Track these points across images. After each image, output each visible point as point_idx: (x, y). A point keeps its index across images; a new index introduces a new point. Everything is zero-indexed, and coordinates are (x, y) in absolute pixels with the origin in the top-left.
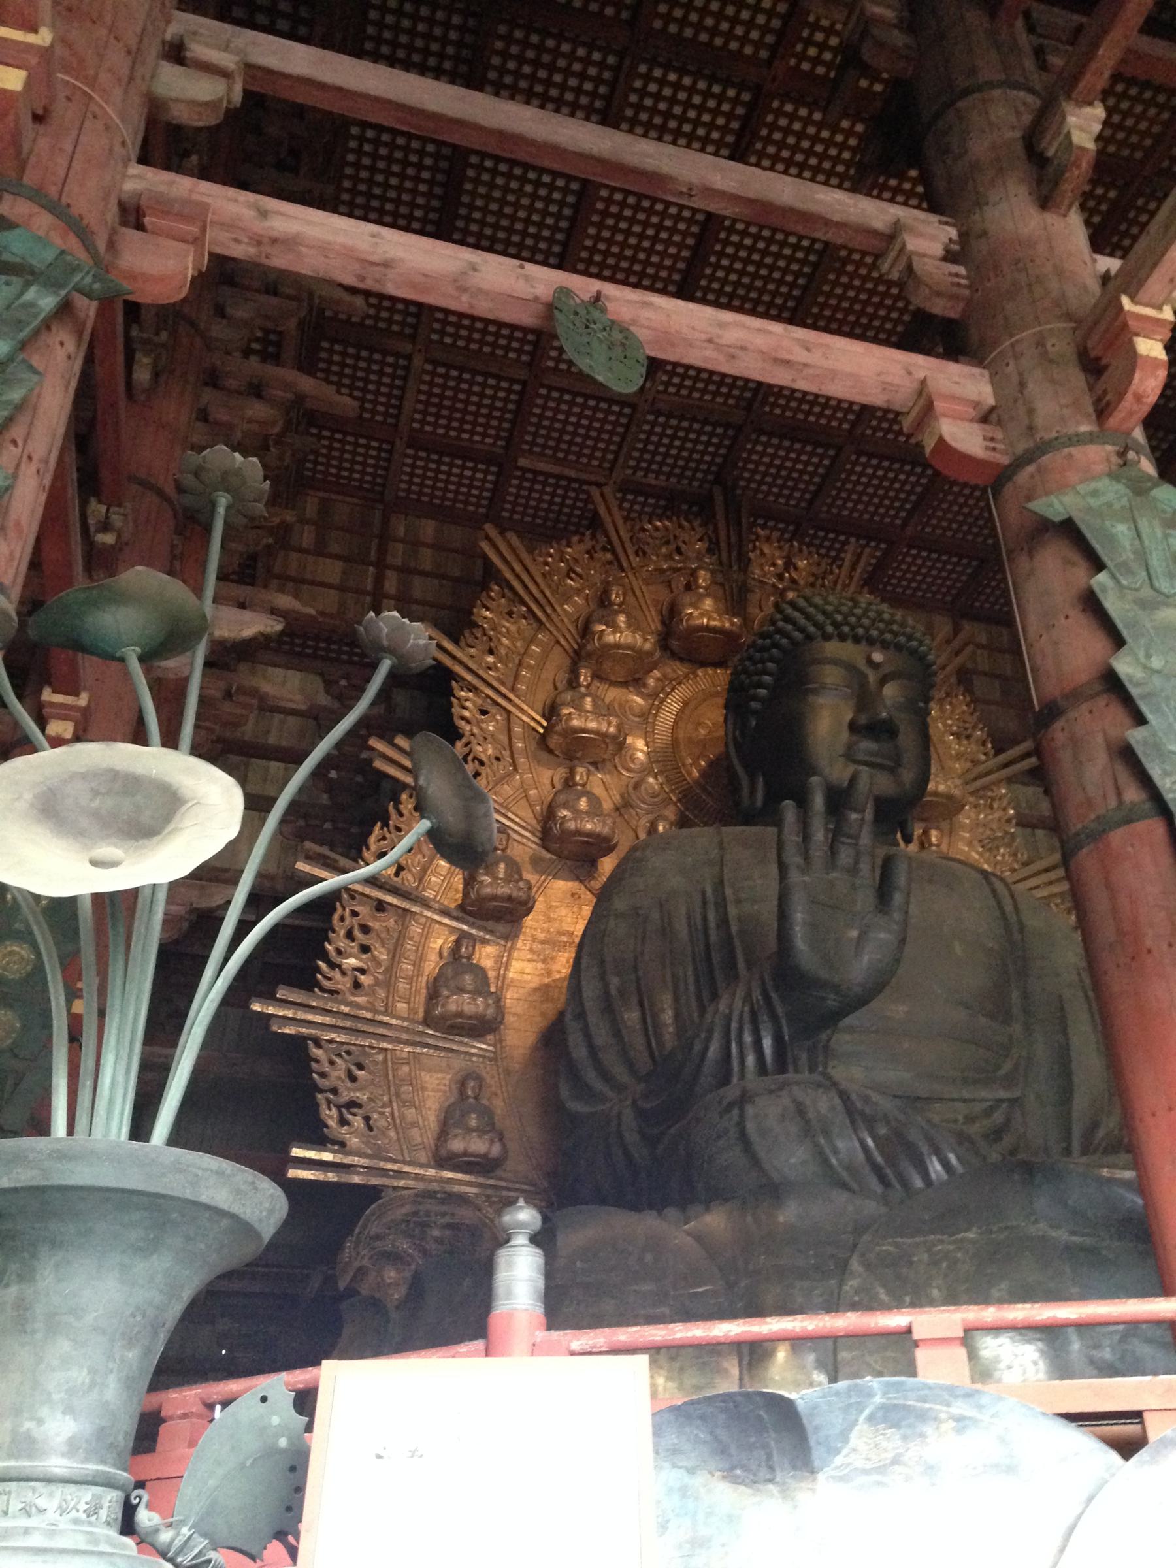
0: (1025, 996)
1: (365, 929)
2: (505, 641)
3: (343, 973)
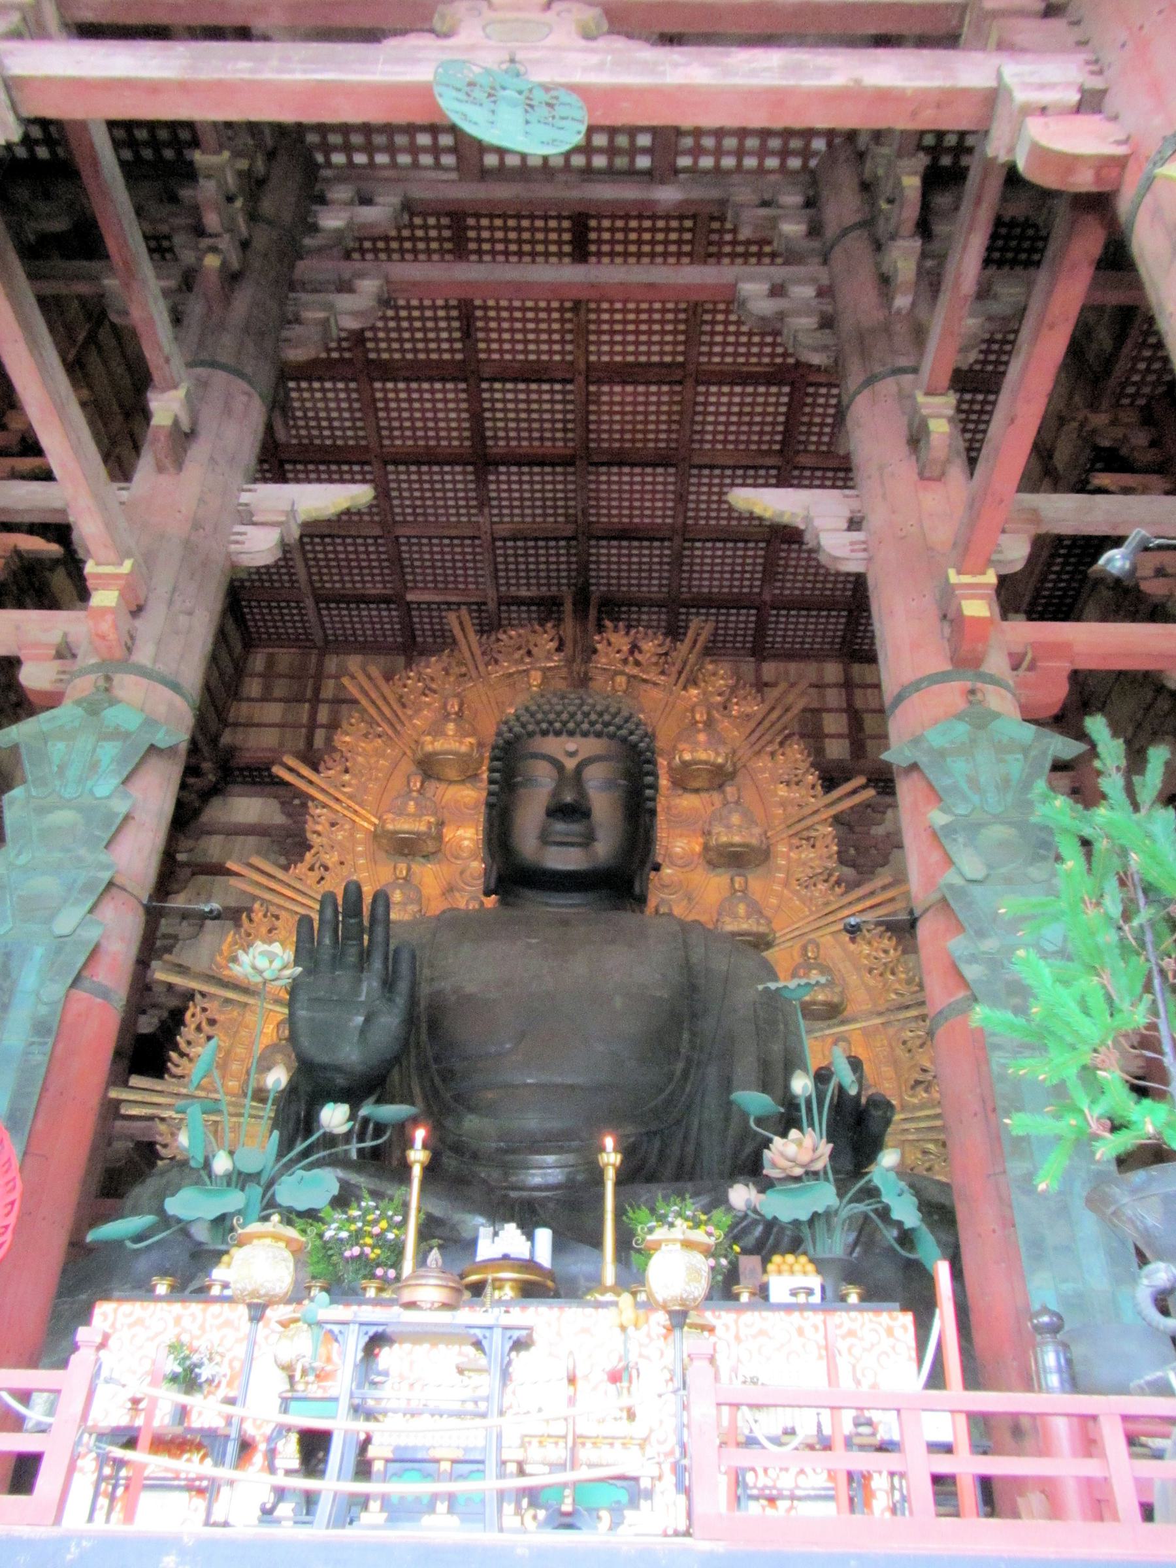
0: (693, 1034)
1: (212, 1022)
2: (360, 759)
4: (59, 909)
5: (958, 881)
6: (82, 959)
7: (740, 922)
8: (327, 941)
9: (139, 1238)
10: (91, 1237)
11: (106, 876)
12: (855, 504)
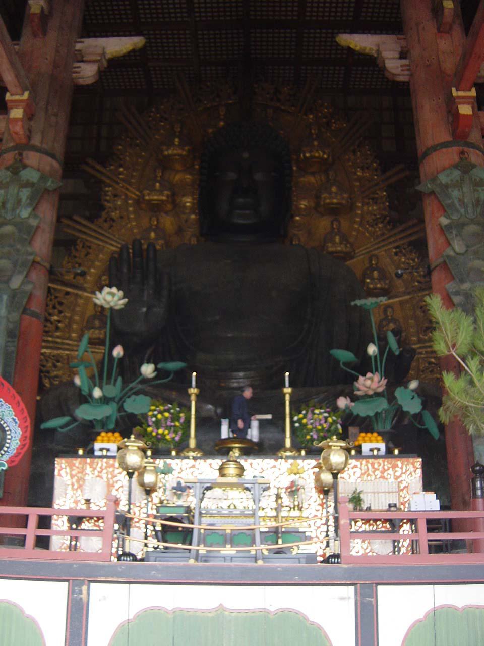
1: (61, 304)
2: (128, 159)
3: (52, 323)
4: (11, 276)
5: (452, 253)
6: (25, 300)
7: (337, 246)
8: (125, 270)
9: (62, 427)
10: (44, 426)
11: (31, 258)
12: (403, 43)
